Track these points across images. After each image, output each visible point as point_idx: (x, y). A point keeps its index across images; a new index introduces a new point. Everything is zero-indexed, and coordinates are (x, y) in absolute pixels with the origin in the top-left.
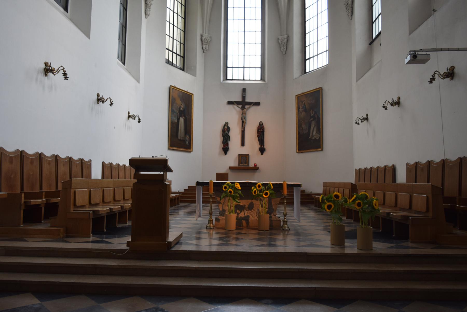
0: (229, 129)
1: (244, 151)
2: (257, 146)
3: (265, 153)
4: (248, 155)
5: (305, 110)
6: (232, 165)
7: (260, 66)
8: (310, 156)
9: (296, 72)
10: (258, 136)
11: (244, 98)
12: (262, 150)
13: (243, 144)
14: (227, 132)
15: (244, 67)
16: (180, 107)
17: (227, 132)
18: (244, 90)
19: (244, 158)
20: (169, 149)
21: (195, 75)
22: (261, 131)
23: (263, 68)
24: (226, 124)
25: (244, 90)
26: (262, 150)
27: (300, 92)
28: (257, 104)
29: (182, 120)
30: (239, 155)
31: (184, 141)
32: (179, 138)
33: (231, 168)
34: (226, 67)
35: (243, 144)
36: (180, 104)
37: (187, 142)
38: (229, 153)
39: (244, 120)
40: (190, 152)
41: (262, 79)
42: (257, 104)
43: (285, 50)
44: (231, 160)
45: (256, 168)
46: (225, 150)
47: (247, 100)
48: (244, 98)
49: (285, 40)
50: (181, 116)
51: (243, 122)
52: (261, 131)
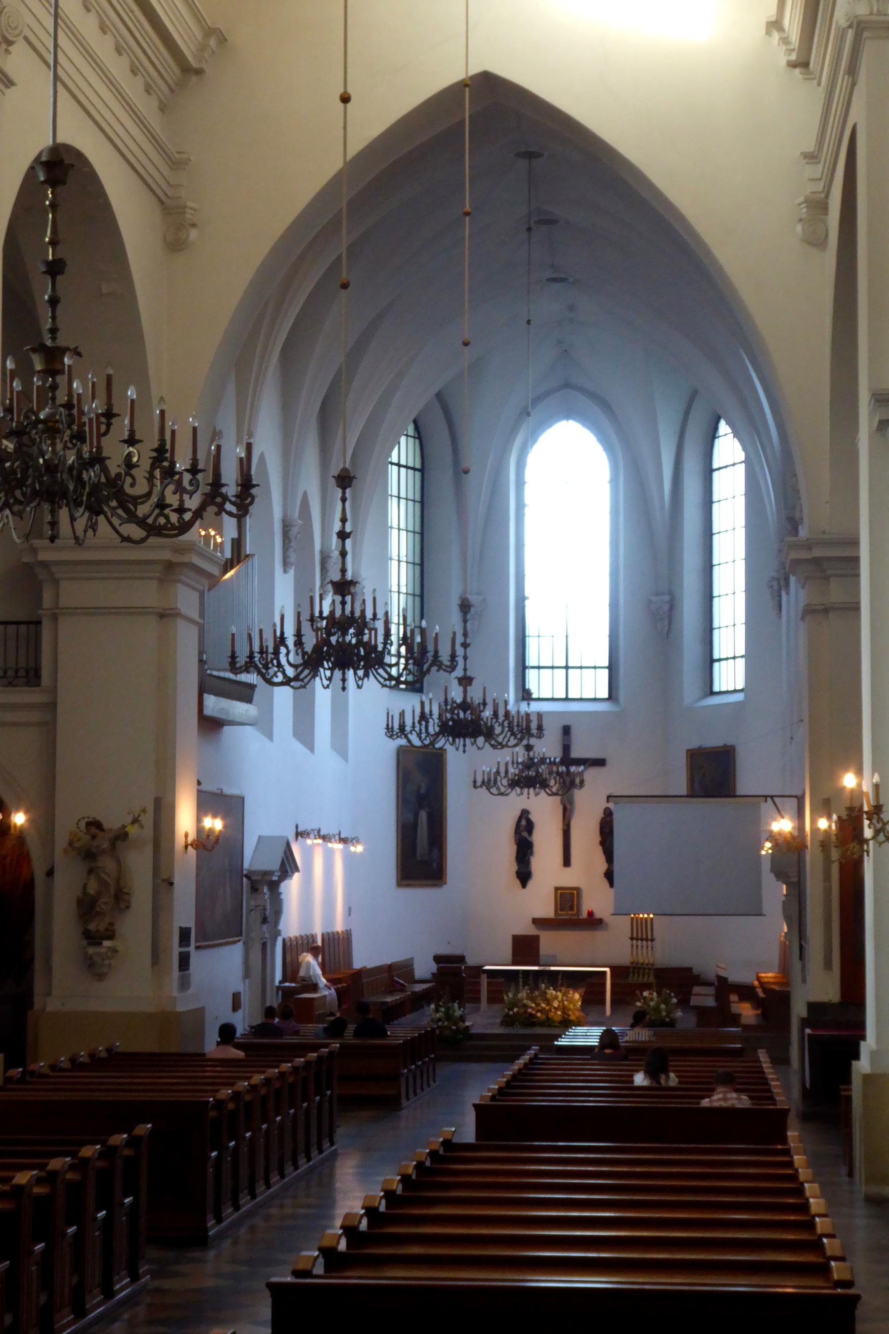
0: (530, 827)
1: (569, 878)
2: (603, 866)
4: (578, 890)
7: (607, 664)
10: (602, 843)
11: (566, 748)
13: (567, 862)
14: (525, 834)
15: (567, 668)
16: (419, 788)
17: (525, 834)
18: (566, 730)
19: (567, 898)
20: (399, 884)
23: (612, 668)
24: (525, 814)
25: (566, 730)
27: (695, 744)
28: (600, 763)
29: (423, 816)
30: (557, 889)
32: (419, 858)
33: (536, 922)
34: (522, 667)
35: (567, 862)
37: (435, 864)
38: (531, 884)
39: (568, 806)
40: (440, 886)
41: (612, 696)
42: (600, 763)
43: (666, 629)
44: (539, 901)
45: (593, 923)
46: (524, 876)
47: (575, 754)
48: (566, 748)
49: (666, 607)
50: (421, 807)
51: (565, 810)
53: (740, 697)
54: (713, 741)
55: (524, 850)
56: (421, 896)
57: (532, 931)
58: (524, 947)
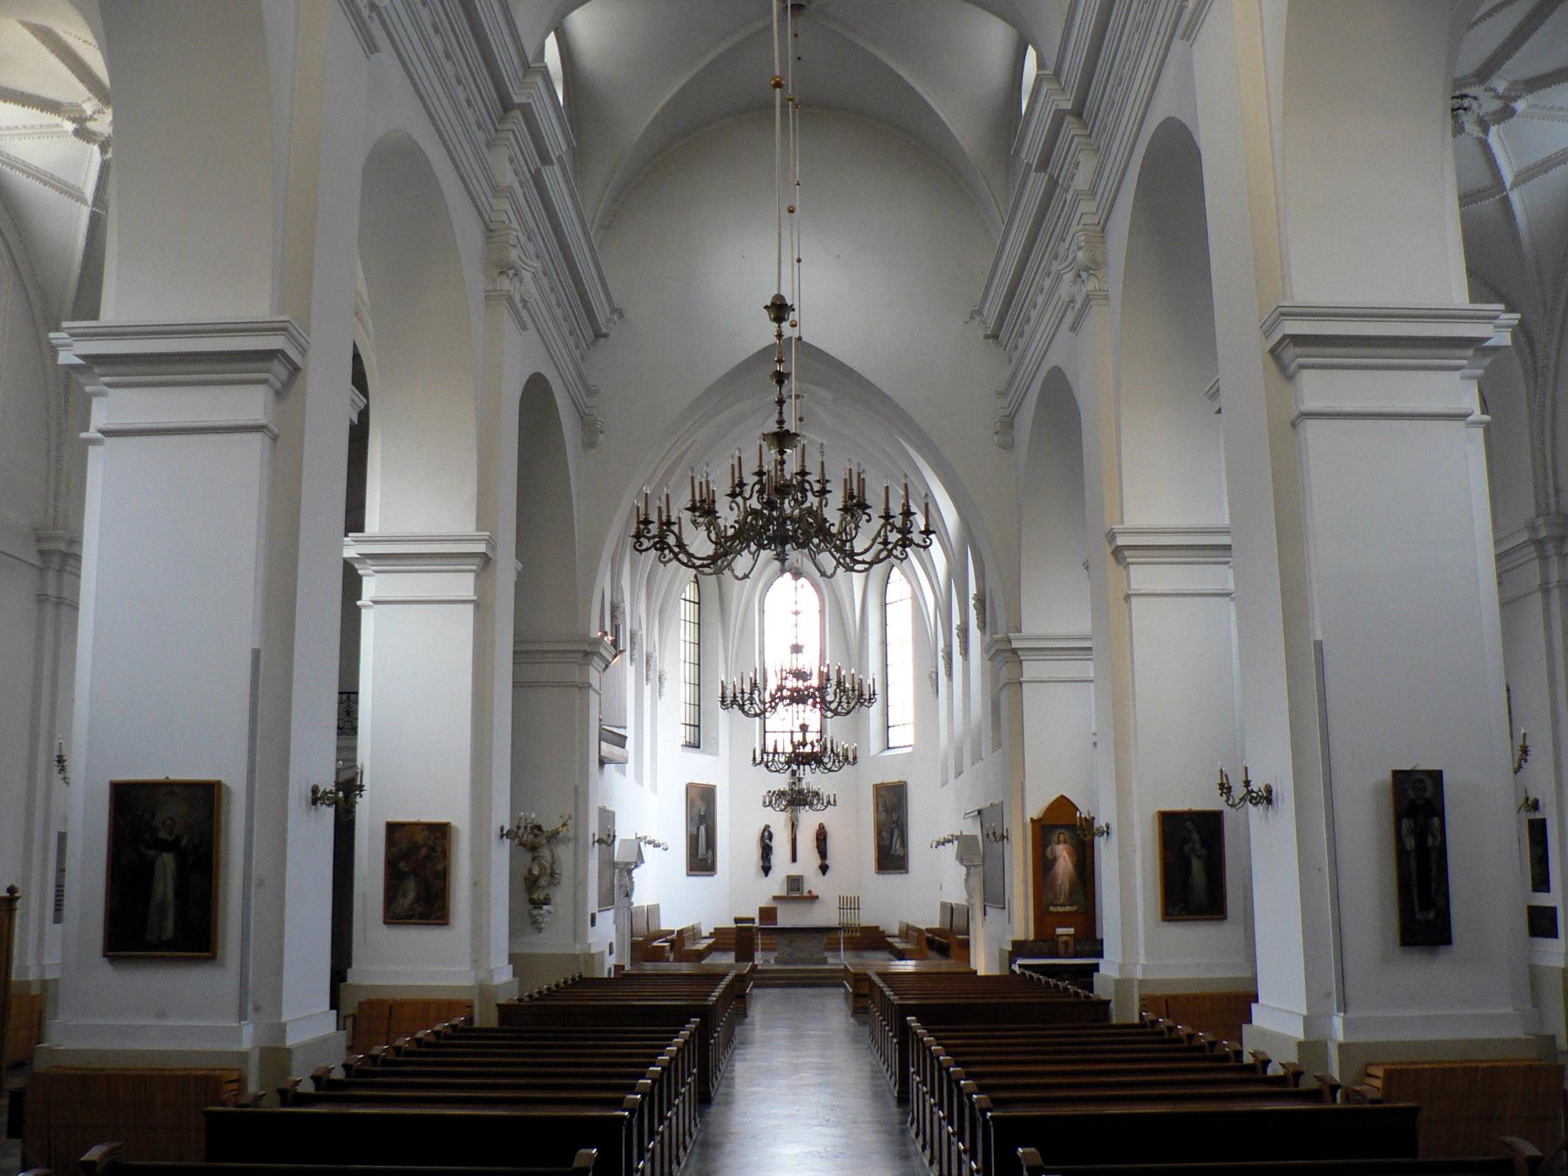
0: (770, 837)
1: (795, 870)
2: (817, 861)
3: (829, 873)
5: (886, 810)
6: (777, 893)
8: (893, 880)
9: (875, 745)
12: (824, 869)
13: (794, 859)
19: (795, 882)
21: (715, 753)
22: (822, 838)
24: (767, 827)
26: (824, 869)
29: (702, 828)
31: (705, 860)
33: (775, 898)
35: (794, 859)
36: (701, 807)
44: (775, 885)
45: (813, 898)
46: (766, 869)
52: (822, 838)
53: (910, 750)
54: (892, 778)
55: (766, 851)
56: (701, 881)
57: (773, 904)
58: (767, 914)
